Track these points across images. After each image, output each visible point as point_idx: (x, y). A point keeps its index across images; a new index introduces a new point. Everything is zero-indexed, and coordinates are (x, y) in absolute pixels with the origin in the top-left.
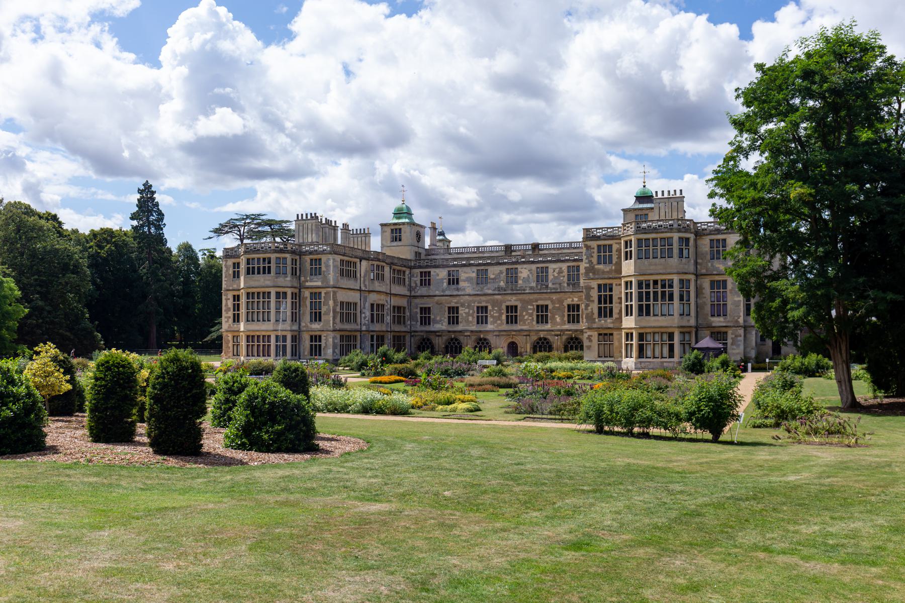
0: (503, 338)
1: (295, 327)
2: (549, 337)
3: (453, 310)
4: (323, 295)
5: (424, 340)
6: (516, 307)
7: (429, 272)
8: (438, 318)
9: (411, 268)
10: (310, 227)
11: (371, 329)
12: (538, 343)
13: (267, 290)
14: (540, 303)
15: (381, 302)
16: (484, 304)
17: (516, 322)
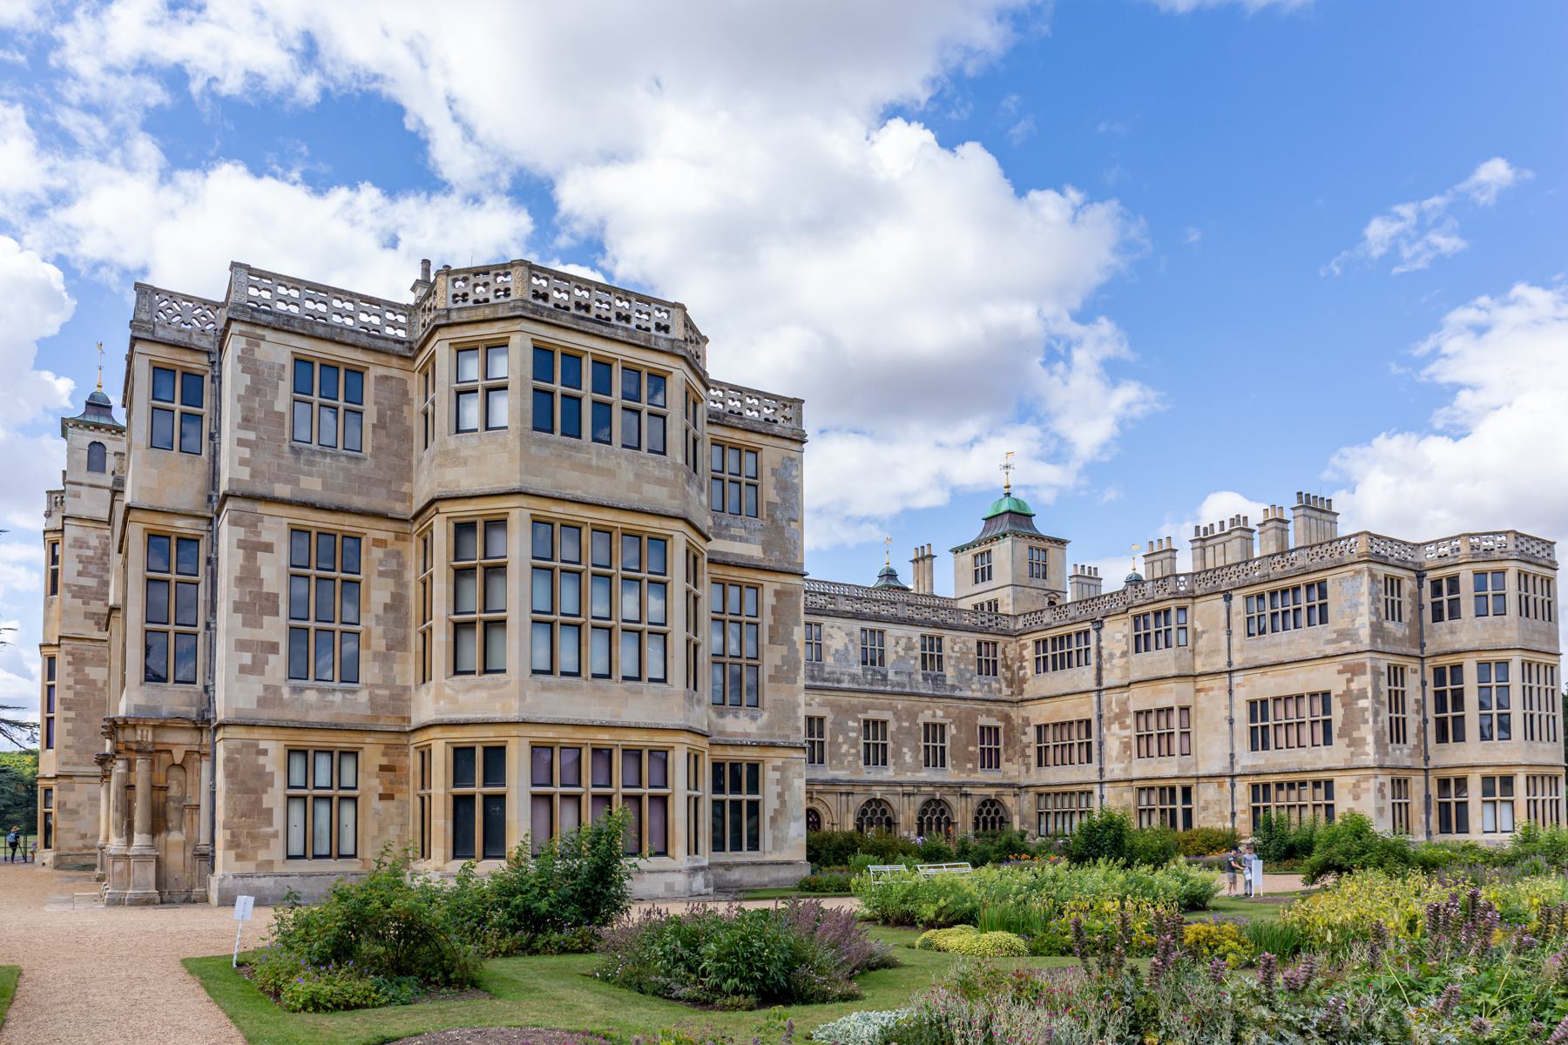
2: (890, 798)
14: (872, 715)
17: (821, 761)
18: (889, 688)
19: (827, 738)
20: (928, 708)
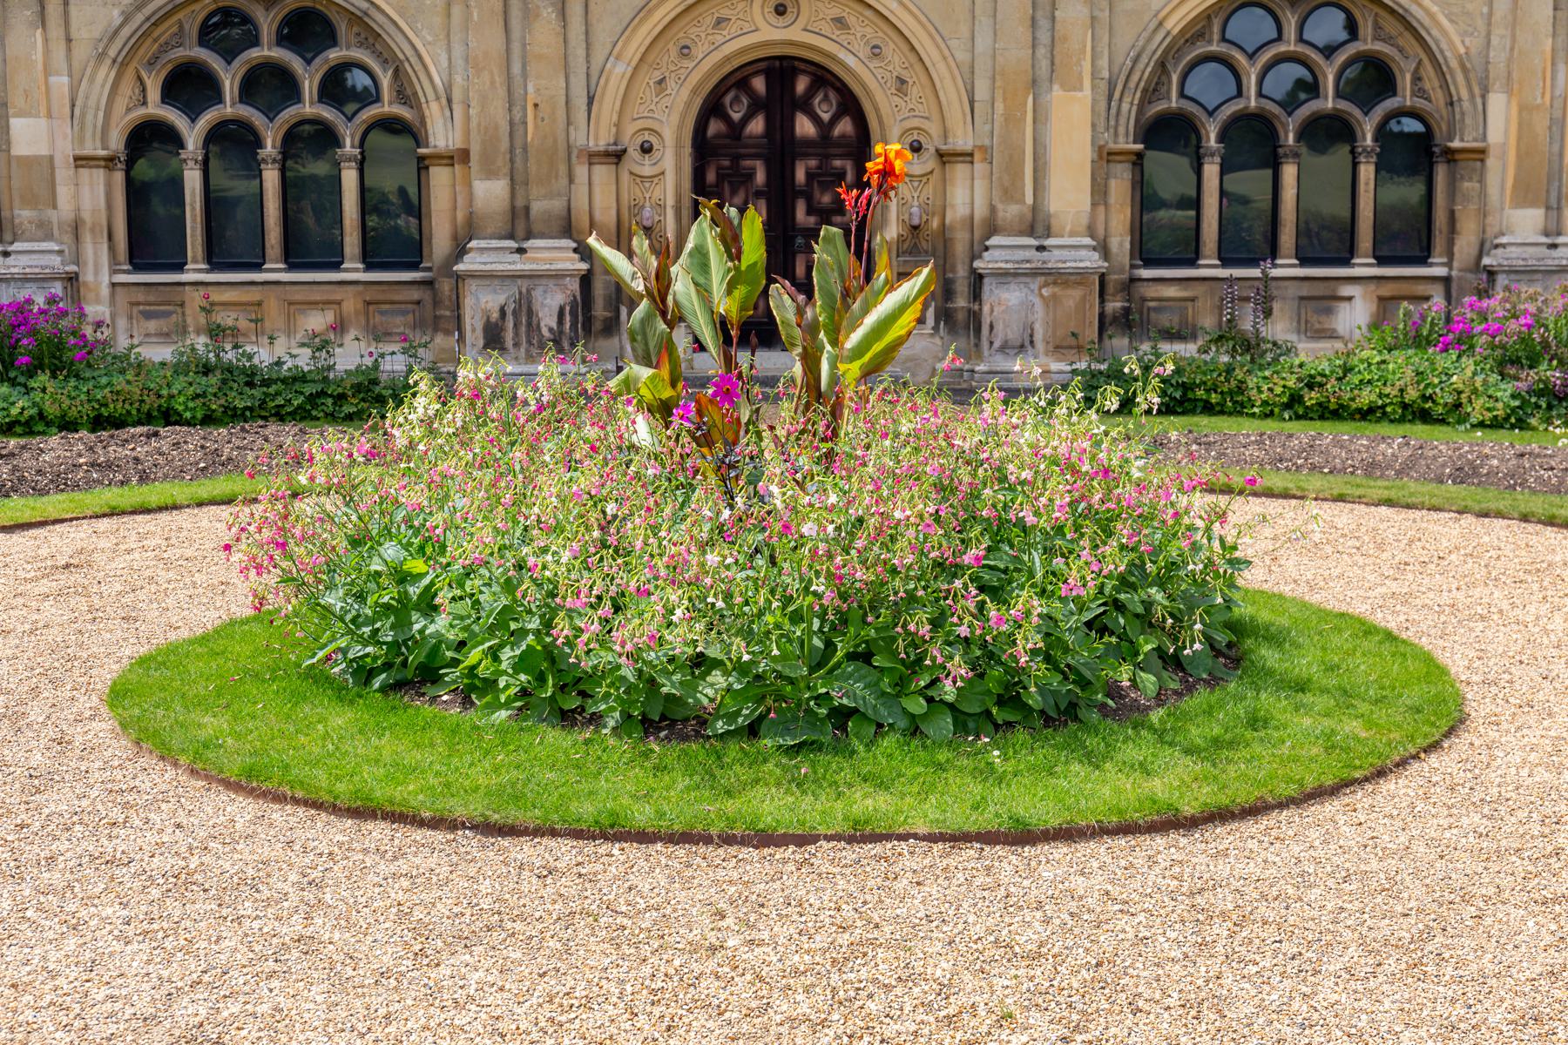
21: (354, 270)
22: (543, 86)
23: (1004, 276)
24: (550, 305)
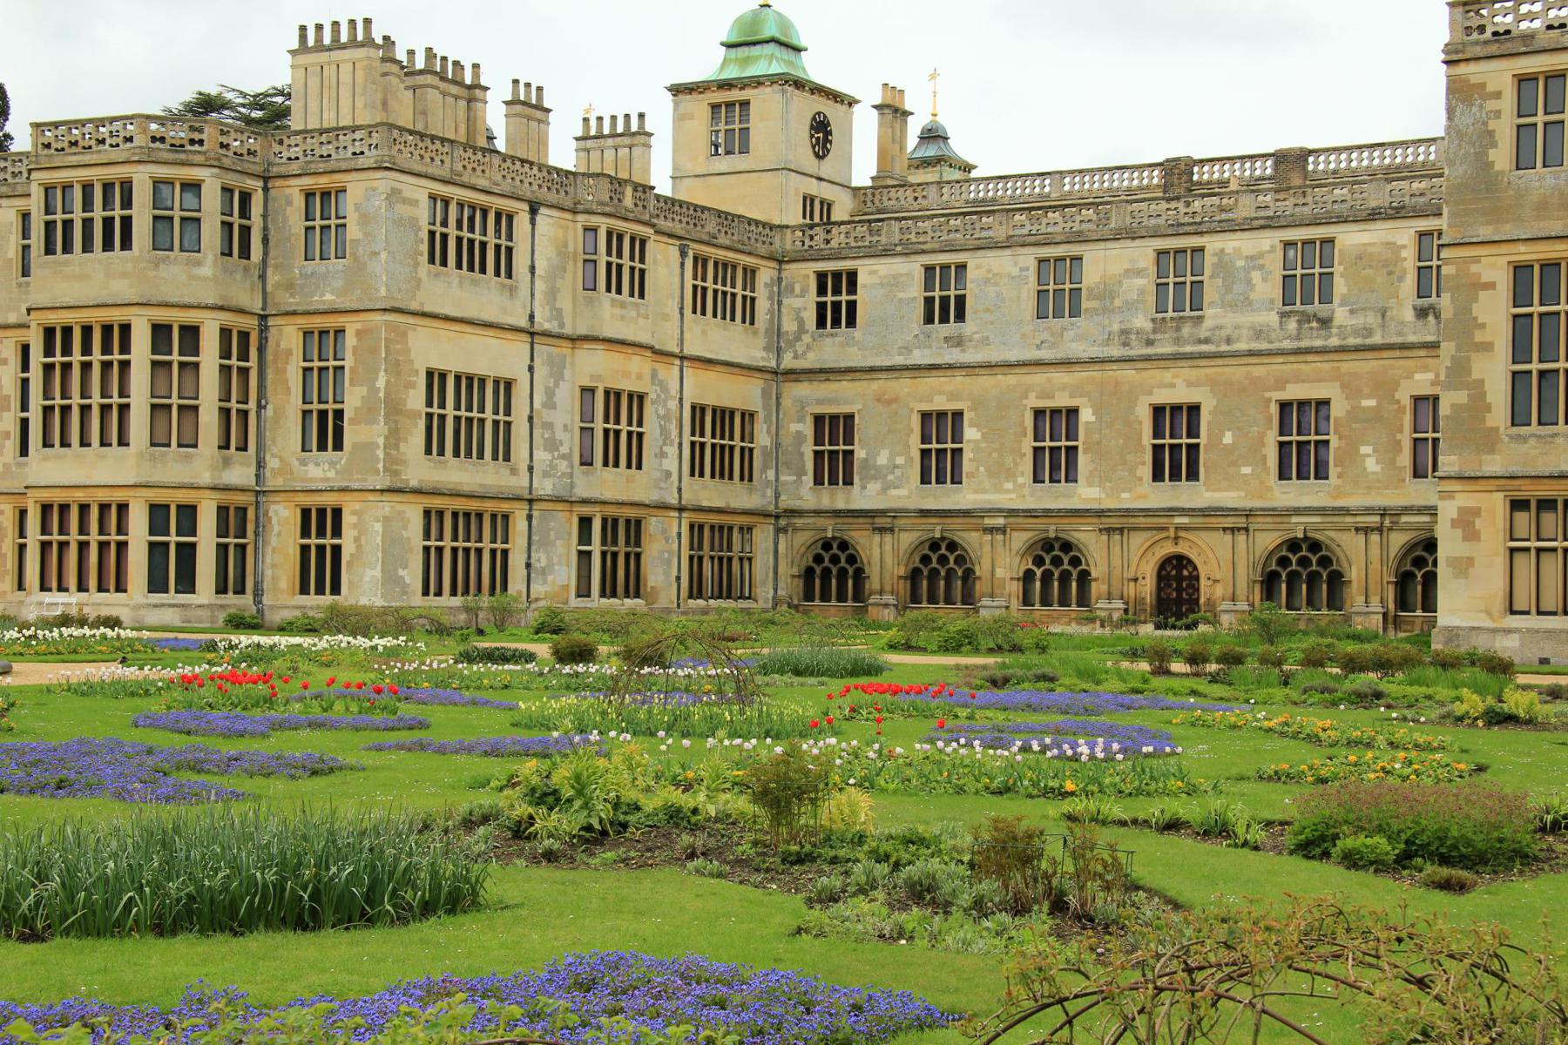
0: (1138, 541)
1: (240, 473)
3: (941, 427)
4: (350, 340)
5: (827, 546)
6: (1194, 409)
7: (852, 276)
8: (882, 460)
9: (780, 261)
10: (346, 76)
11: (581, 491)
12: (1284, 562)
13: (116, 316)
14: (1294, 392)
15: (627, 385)
16: (1062, 401)
17: (1193, 475)
18: (1334, 342)
19: (1202, 440)
20: (1426, 369)
21: (1074, 607)
22: (1116, 562)
23: (1225, 611)
24: (1116, 616)
